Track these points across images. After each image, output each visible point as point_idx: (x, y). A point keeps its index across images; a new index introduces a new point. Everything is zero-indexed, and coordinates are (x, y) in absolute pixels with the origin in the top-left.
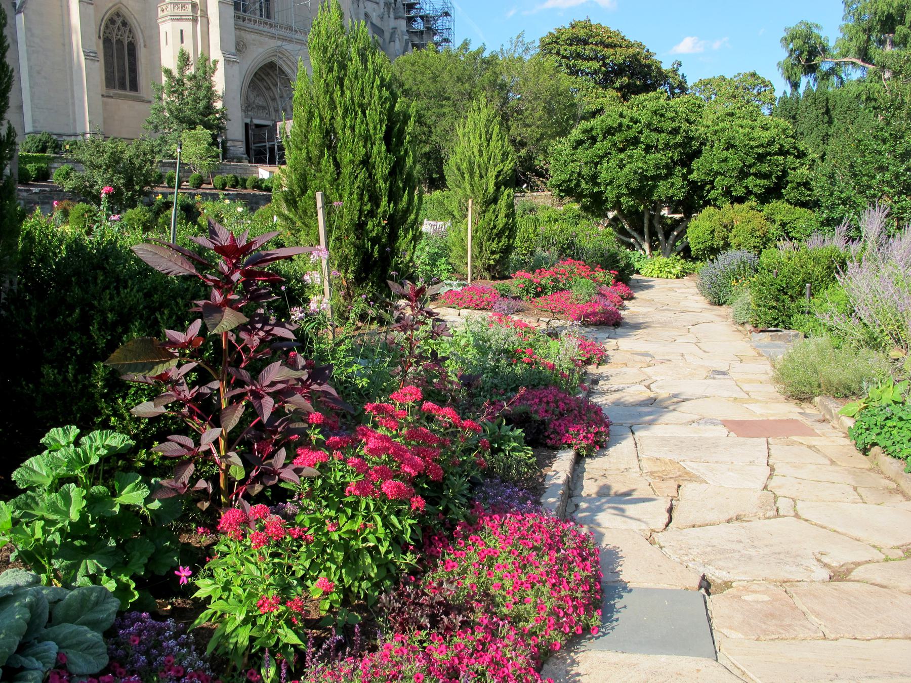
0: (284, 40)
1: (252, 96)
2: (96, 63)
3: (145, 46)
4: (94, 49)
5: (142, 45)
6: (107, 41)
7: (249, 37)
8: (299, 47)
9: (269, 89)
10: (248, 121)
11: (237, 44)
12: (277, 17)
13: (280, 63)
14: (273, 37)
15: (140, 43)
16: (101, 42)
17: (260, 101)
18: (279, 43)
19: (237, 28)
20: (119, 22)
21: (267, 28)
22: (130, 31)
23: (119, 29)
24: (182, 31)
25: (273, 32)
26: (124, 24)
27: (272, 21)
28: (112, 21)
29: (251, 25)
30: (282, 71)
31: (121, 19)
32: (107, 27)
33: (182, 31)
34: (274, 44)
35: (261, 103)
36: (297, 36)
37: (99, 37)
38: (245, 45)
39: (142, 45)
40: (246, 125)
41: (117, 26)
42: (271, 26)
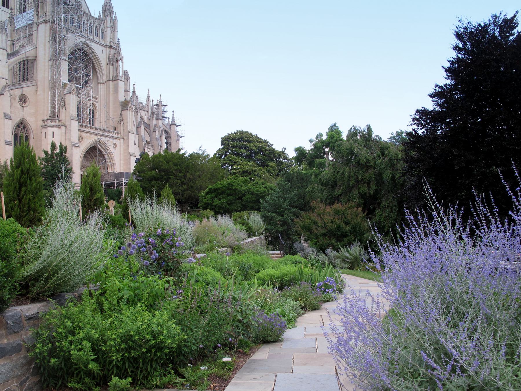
0: (101, 135)
1: (84, 162)
2: (11, 146)
3: (33, 138)
4: (10, 140)
5: (32, 137)
6: (16, 136)
7: (84, 135)
8: (108, 139)
9: (93, 158)
10: (82, 173)
11: (79, 138)
12: (98, 125)
13: (98, 146)
14: (96, 134)
15: (31, 136)
16: (13, 136)
17: (88, 164)
18: (99, 137)
19: (80, 131)
20: (22, 126)
21: (93, 131)
22: (27, 131)
23: (21, 130)
24: (53, 132)
25: (96, 132)
26: (24, 127)
27: (97, 127)
28: (19, 126)
29: (85, 129)
30: (100, 150)
31: (23, 125)
32: (16, 129)
33: (53, 132)
34: (96, 138)
35: (88, 165)
36: (107, 134)
37: (12, 134)
38: (82, 138)
39: (32, 137)
40: (81, 175)
41: (20, 128)
42: (95, 130)
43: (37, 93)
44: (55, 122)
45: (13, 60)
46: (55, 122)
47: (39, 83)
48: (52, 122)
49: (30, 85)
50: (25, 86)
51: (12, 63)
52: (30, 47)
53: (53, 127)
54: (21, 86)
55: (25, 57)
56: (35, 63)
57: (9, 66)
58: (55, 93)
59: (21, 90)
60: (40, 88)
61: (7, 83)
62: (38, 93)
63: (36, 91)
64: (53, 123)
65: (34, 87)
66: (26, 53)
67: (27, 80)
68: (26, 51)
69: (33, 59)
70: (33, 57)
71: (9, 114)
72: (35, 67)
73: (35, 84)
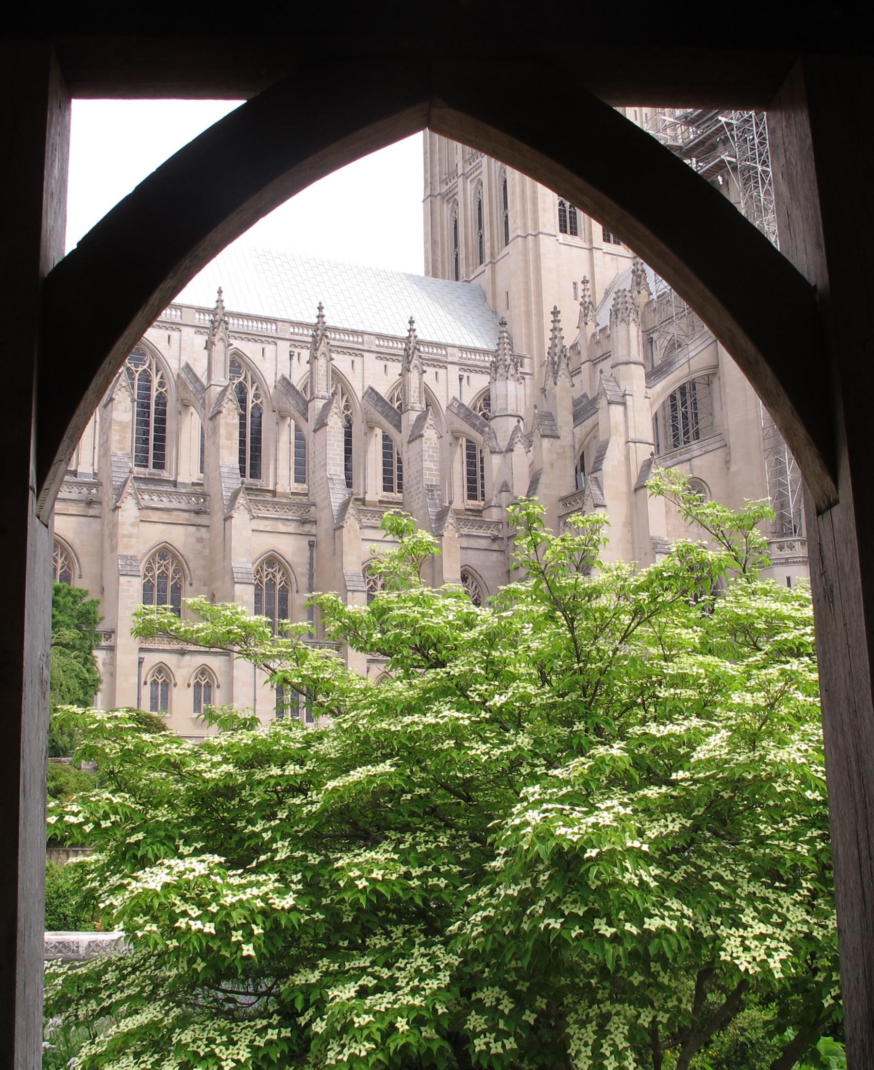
43: (728, 469)
44: (791, 547)
45: (659, 387)
46: (791, 547)
47: (732, 440)
48: (781, 548)
49: (710, 448)
50: (696, 453)
51: (659, 395)
52: (698, 342)
53: (786, 562)
54: (687, 456)
55: (689, 374)
56: (715, 385)
57: (651, 405)
58: (781, 463)
59: (686, 466)
60: (736, 455)
61: (652, 454)
62: (733, 468)
63: (727, 462)
64: (787, 553)
65: (720, 454)
66: (691, 362)
67: (697, 436)
68: (692, 354)
69: (708, 375)
70: (708, 368)
71: (666, 539)
72: (716, 395)
73: (722, 443)
